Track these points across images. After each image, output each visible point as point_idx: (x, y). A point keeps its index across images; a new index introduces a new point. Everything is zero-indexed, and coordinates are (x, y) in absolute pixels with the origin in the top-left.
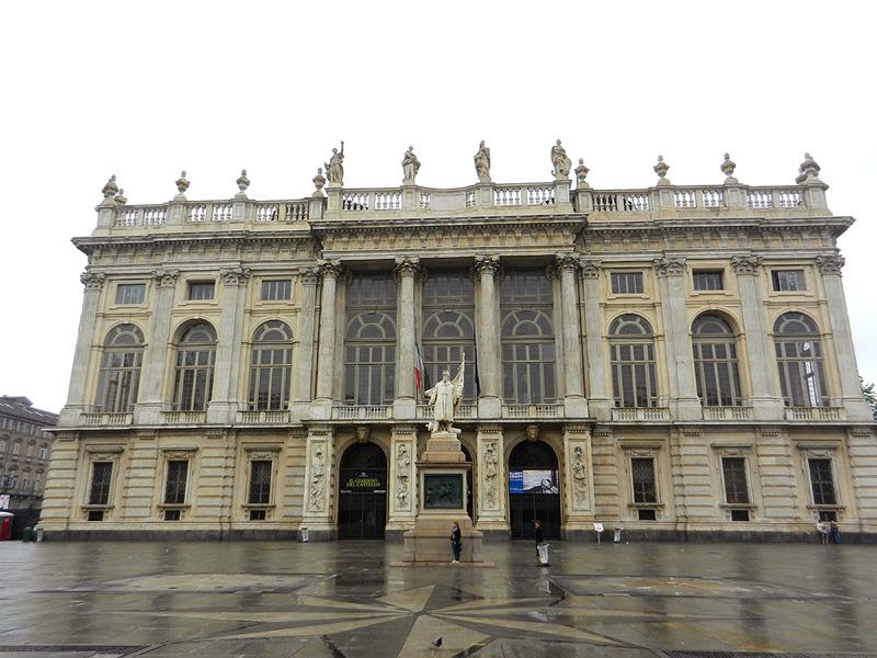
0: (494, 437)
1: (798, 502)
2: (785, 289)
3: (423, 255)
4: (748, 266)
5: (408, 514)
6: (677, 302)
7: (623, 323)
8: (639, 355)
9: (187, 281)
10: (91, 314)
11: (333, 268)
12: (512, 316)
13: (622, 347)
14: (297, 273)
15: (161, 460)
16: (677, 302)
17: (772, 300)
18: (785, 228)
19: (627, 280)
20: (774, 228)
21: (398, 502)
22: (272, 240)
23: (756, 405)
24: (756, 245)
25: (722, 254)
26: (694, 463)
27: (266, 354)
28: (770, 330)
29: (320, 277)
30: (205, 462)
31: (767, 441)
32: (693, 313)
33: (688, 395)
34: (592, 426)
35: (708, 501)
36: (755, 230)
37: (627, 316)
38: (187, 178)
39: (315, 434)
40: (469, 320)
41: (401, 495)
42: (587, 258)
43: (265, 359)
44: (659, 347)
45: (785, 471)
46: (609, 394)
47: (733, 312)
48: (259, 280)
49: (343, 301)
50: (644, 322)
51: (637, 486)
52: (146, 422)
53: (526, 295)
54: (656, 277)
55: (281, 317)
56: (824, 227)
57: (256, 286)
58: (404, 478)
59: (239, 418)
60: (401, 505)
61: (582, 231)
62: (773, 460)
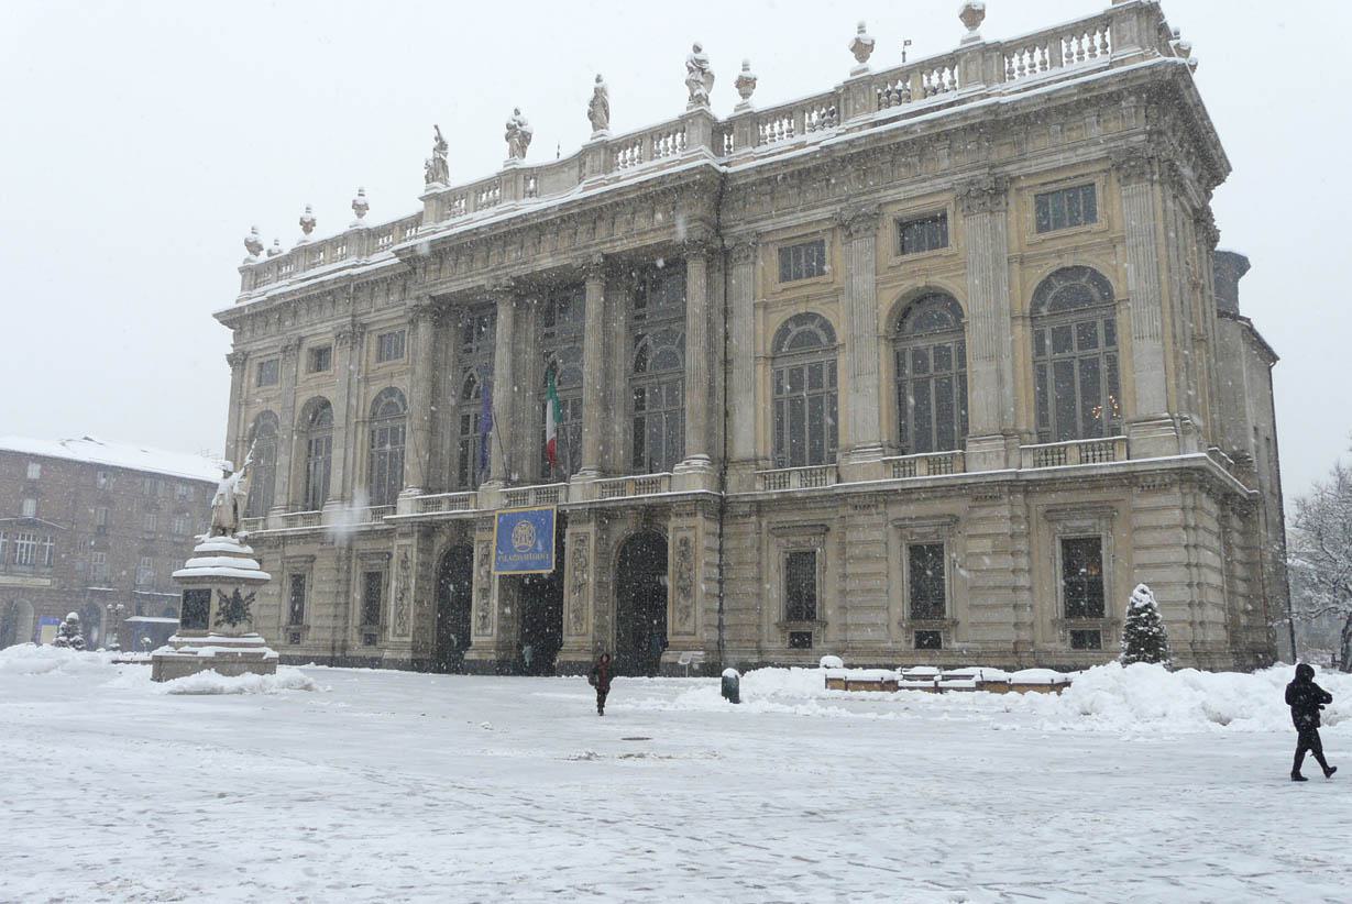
0: (581, 529)
1: (1026, 616)
2: (1059, 224)
3: (521, 271)
4: (992, 193)
5: (488, 639)
6: (863, 283)
7: (795, 330)
8: (815, 383)
9: (312, 350)
10: (239, 400)
11: (425, 310)
15: (286, 573)
16: (863, 283)
19: (802, 258)
20: (1027, 116)
21: (479, 624)
24: (1006, 152)
25: (942, 183)
31: (983, 512)
32: (889, 298)
35: (881, 618)
36: (1000, 125)
37: (799, 319)
38: (313, 215)
39: (404, 535)
41: (481, 614)
42: (741, 228)
44: (843, 360)
45: (1007, 562)
46: (765, 446)
48: (374, 339)
49: (449, 353)
50: (828, 328)
55: (396, 383)
57: (371, 343)
60: (484, 627)
61: (718, 191)
62: (987, 544)
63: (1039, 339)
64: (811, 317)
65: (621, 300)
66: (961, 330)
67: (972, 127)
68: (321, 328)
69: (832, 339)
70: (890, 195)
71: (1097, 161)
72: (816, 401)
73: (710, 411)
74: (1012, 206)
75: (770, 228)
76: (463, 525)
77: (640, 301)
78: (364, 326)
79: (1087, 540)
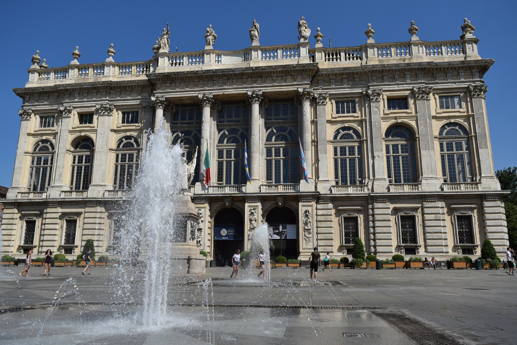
7: (342, 133)
11: (161, 102)
13: (341, 148)
14: (141, 106)
17: (438, 115)
18: (448, 68)
20: (440, 69)
22: (126, 87)
23: (424, 182)
26: (382, 219)
27: (124, 156)
30: (86, 221)
34: (317, 197)
37: (344, 129)
40: (245, 133)
47: (413, 123)
51: (347, 234)
52: (53, 197)
53: (282, 116)
54: (363, 102)
56: (474, 67)
59: (107, 195)
62: (433, 217)
63: (441, 145)
64: (349, 128)
67: (421, 69)
72: (352, 161)
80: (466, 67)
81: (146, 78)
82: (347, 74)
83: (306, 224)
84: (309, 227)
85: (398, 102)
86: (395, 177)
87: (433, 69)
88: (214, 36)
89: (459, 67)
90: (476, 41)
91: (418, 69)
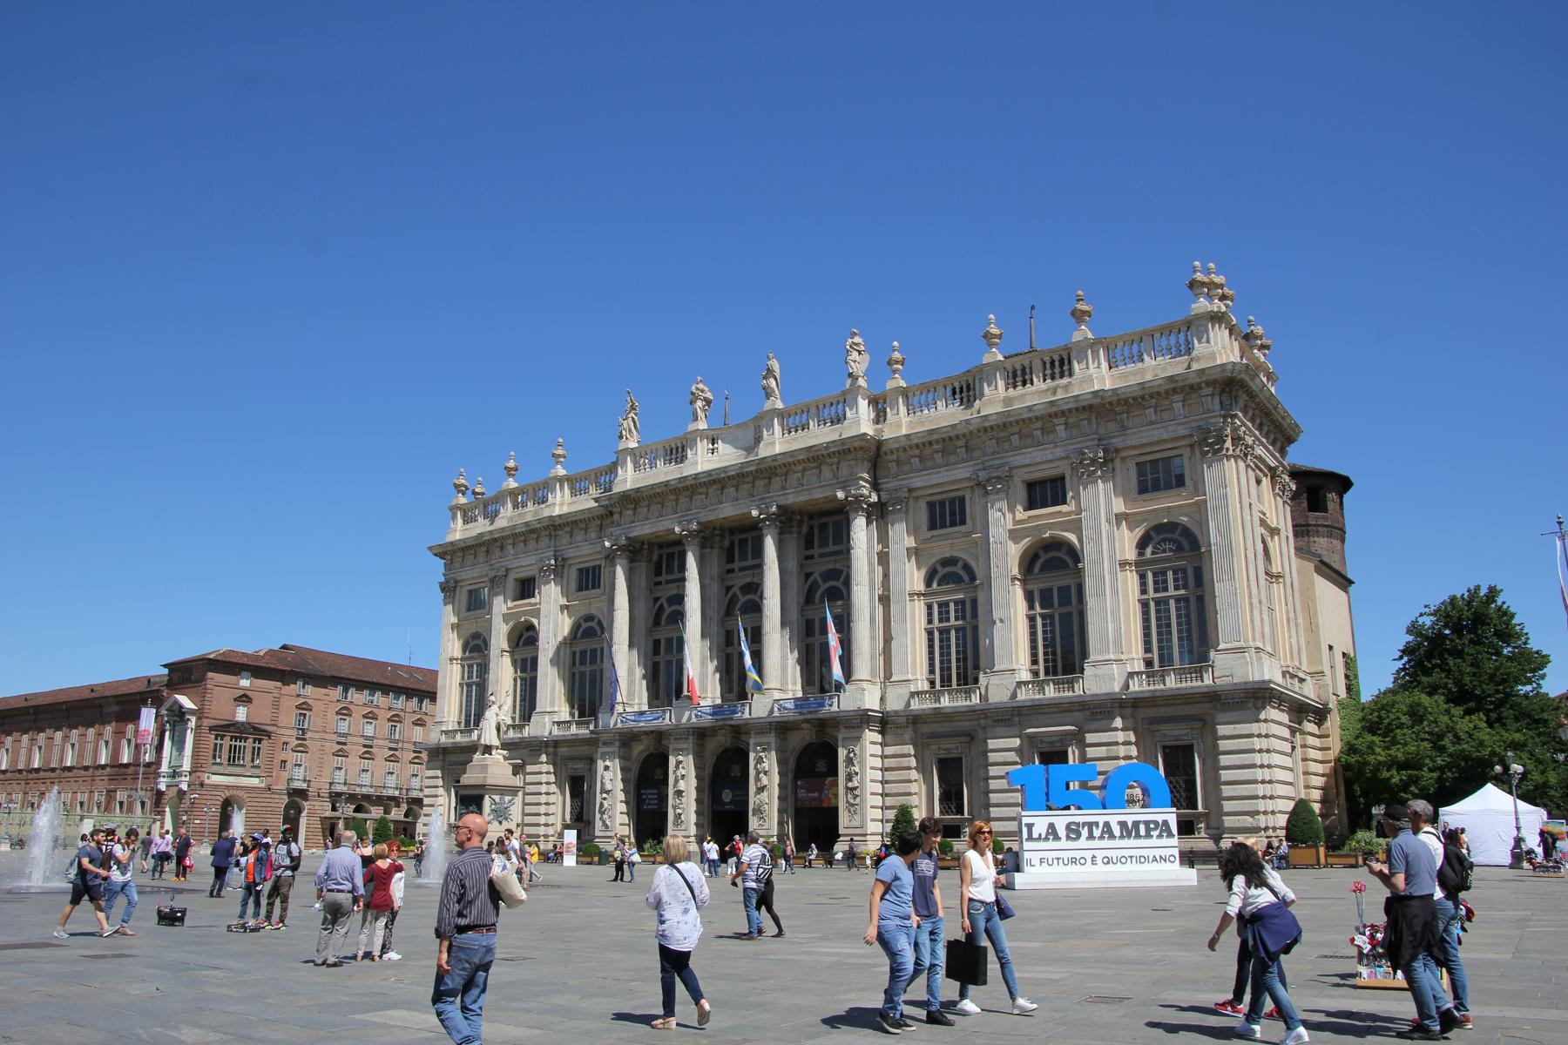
0: (766, 740)
2: (1156, 488)
12: (815, 581)
18: (1143, 397)
20: (1126, 401)
25: (1059, 452)
28: (1131, 554)
29: (610, 557)
33: (1002, 667)
39: (605, 744)
42: (894, 484)
43: (583, 663)
47: (1073, 538)
58: (679, 793)
61: (874, 455)
62: (1101, 751)
65: (793, 543)
66: (1079, 573)
67: (1084, 408)
68: (526, 561)
69: (973, 578)
70: (1018, 460)
71: (1184, 437)
73: (873, 638)
74: (1118, 471)
75: (919, 484)
76: (659, 735)
77: (809, 543)
78: (564, 560)
79: (1184, 747)
80: (1182, 389)
81: (593, 504)
82: (937, 442)
83: (849, 778)
84: (855, 783)
85: (1045, 492)
86: (1046, 661)
87: (1111, 404)
88: (705, 399)
89: (1167, 392)
90: (1218, 318)
91: (1077, 409)
